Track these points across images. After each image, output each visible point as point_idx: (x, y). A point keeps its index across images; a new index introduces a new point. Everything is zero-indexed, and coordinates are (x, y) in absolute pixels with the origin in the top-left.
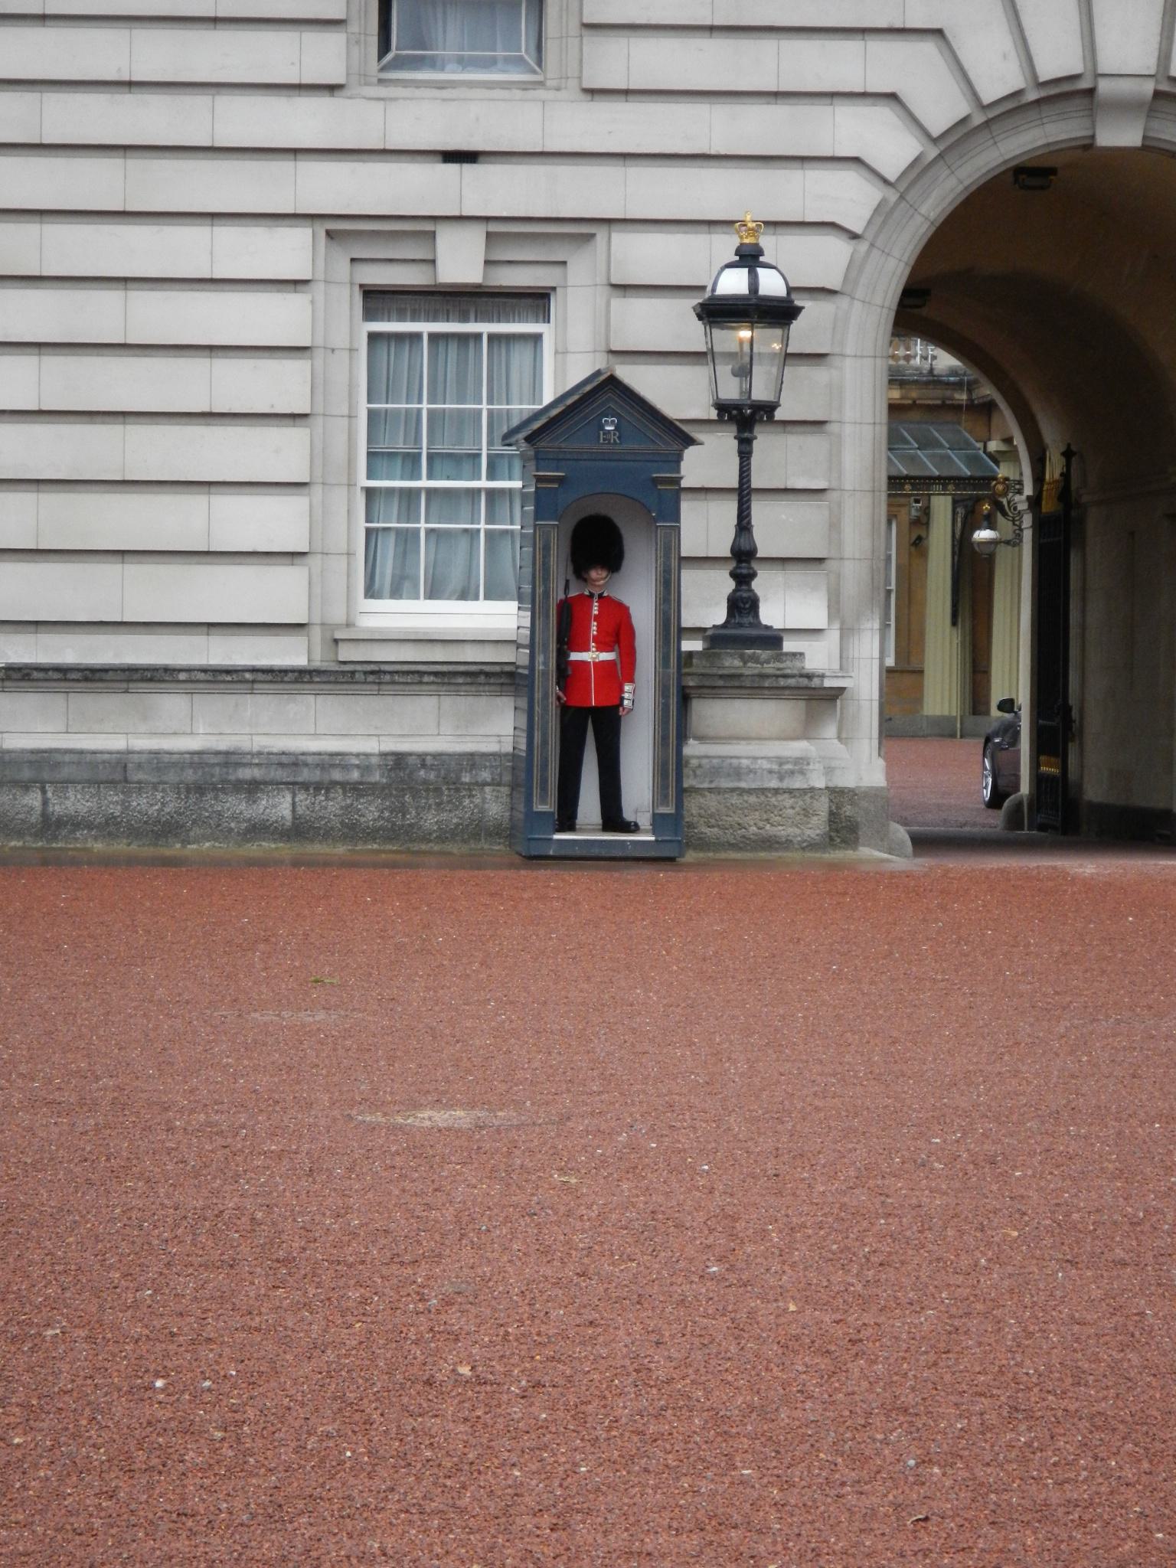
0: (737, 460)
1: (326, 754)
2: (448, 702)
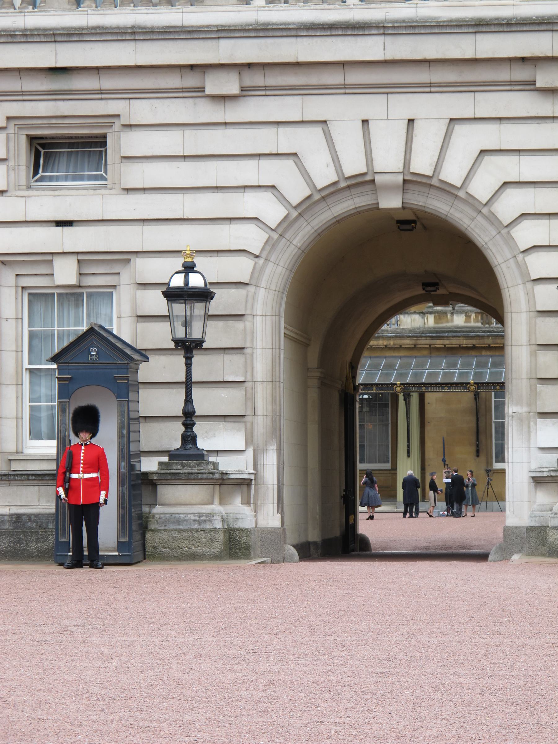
0: (184, 368)
2: (43, 488)
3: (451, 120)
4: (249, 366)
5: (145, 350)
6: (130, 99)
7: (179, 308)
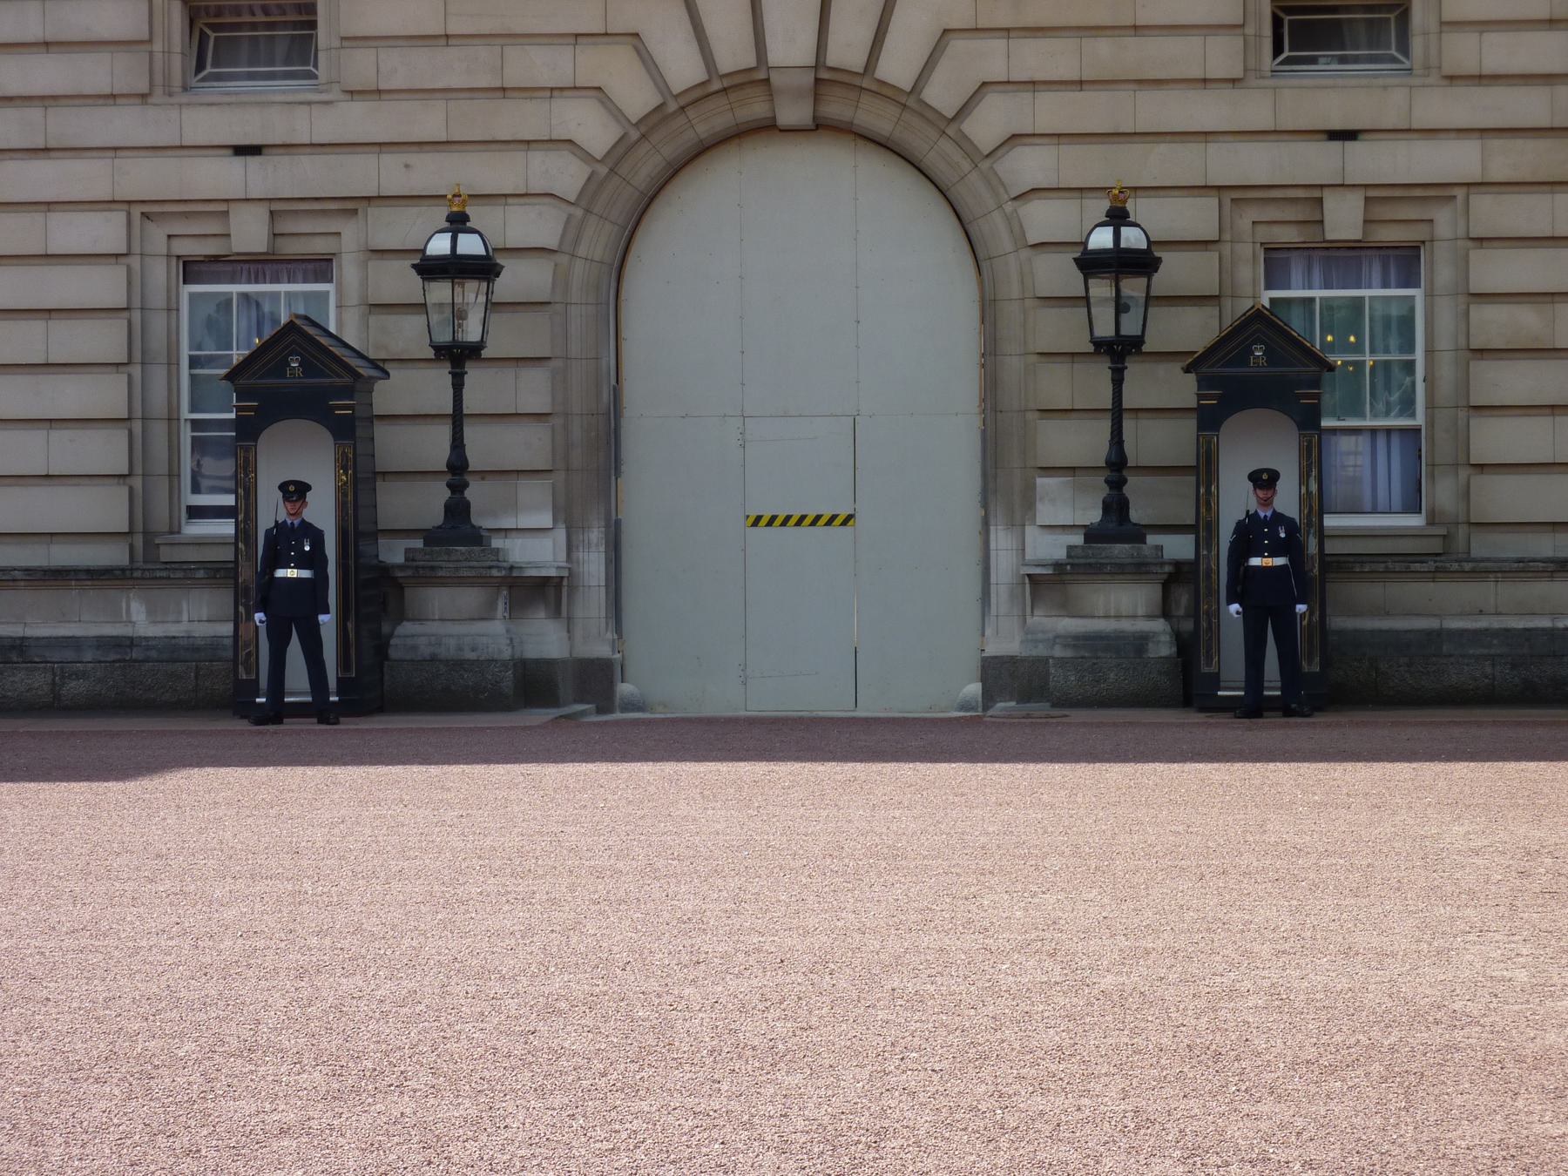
0: (451, 391)
5: (384, 360)
7: (440, 291)
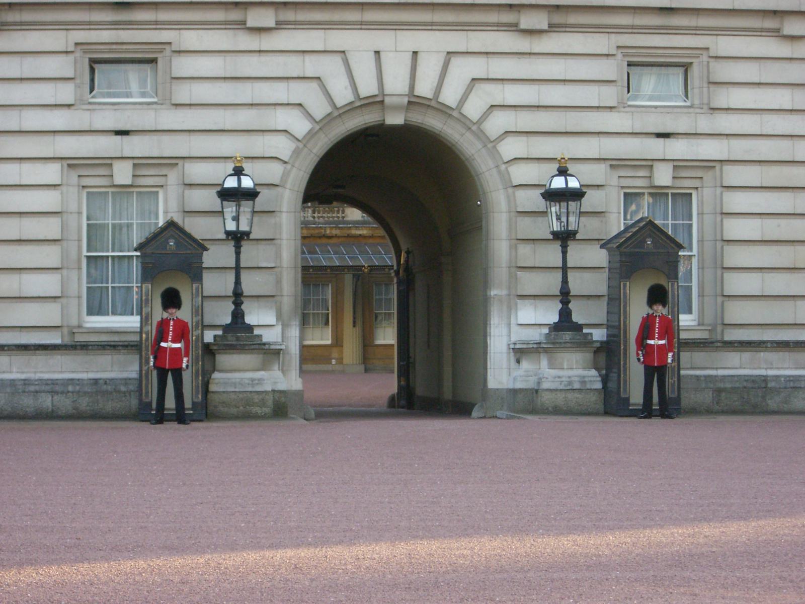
0: (234, 256)
1: (65, 379)
3: (448, 53)
4: (278, 255)
5: (205, 240)
6: (180, 29)
